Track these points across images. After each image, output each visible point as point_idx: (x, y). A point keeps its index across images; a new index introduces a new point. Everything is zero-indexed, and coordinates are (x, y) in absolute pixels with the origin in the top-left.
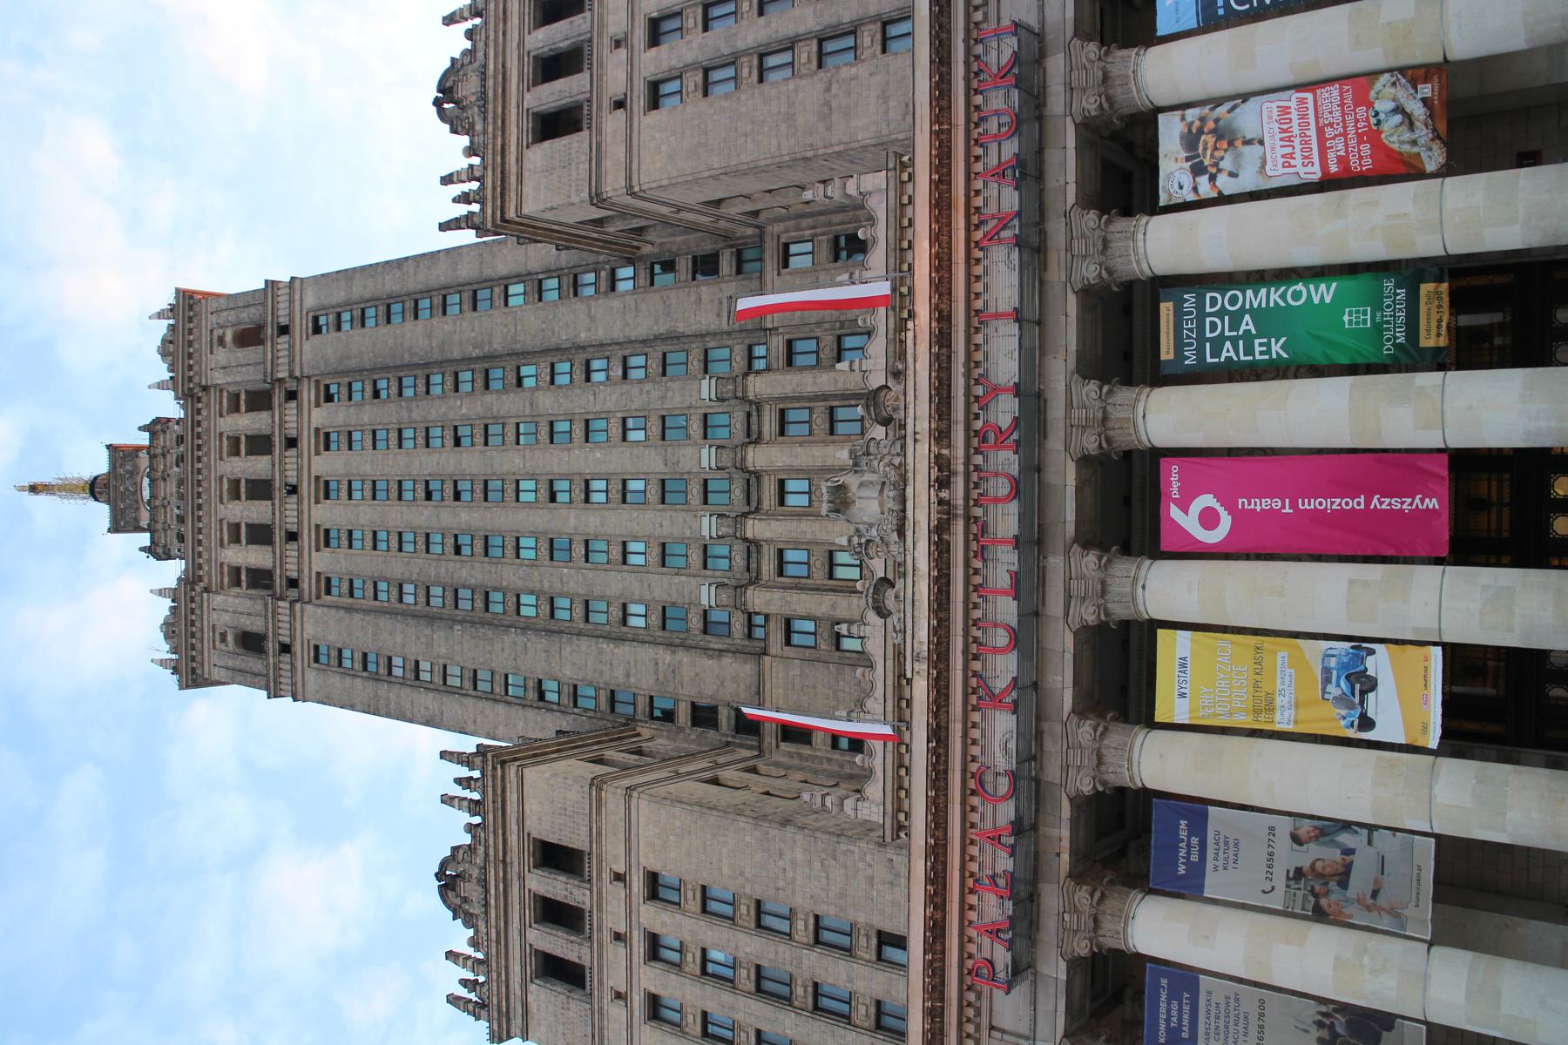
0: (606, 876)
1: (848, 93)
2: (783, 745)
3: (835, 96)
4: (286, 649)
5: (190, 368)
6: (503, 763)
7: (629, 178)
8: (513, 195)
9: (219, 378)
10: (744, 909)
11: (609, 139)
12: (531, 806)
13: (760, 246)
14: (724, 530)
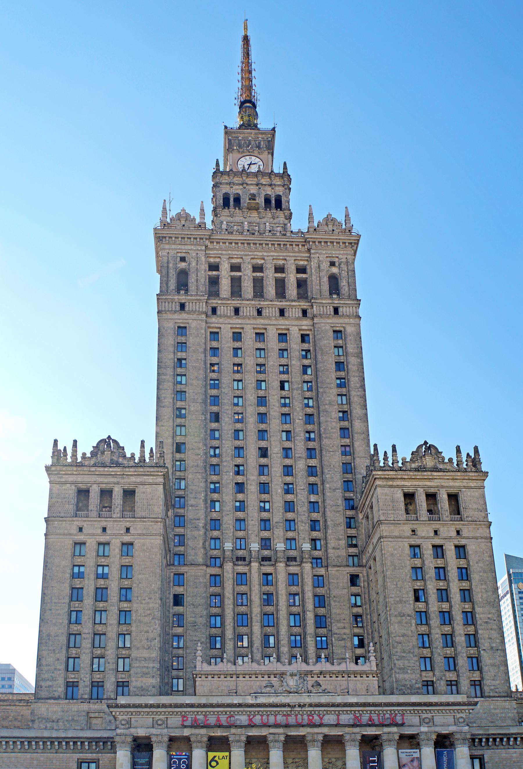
0: (128, 525)
1: (406, 623)
3: (406, 618)
7: (386, 537)
8: (385, 483)
9: (314, 264)
10: (126, 583)
11: (401, 528)
12: (148, 488)
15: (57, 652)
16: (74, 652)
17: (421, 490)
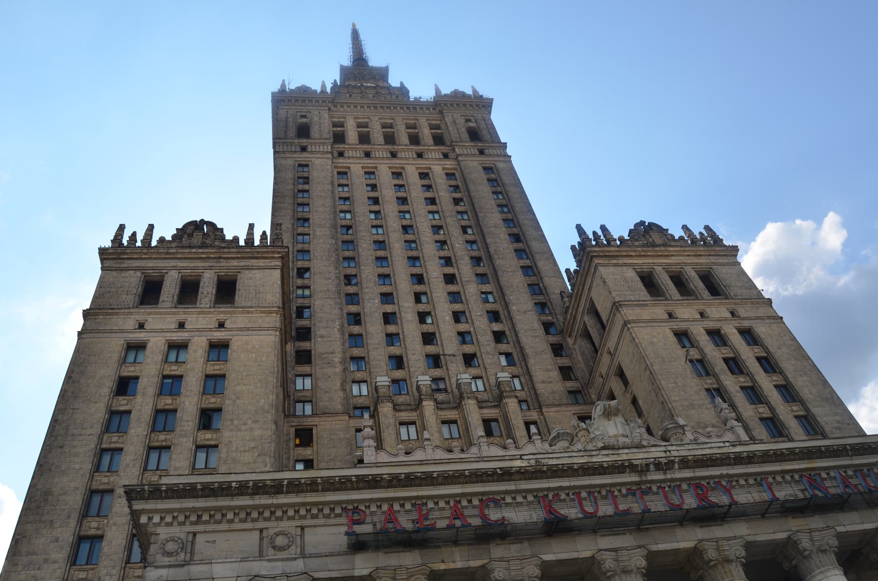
0: (221, 317)
2: (293, 430)
4: (304, 149)
5: (452, 105)
6: (282, 258)
7: (634, 321)
8: (606, 262)
9: (449, 119)
11: (651, 311)
12: (258, 274)
13: (585, 404)
14: (424, 389)
15: (57, 525)
16: (94, 524)
17: (659, 269)
